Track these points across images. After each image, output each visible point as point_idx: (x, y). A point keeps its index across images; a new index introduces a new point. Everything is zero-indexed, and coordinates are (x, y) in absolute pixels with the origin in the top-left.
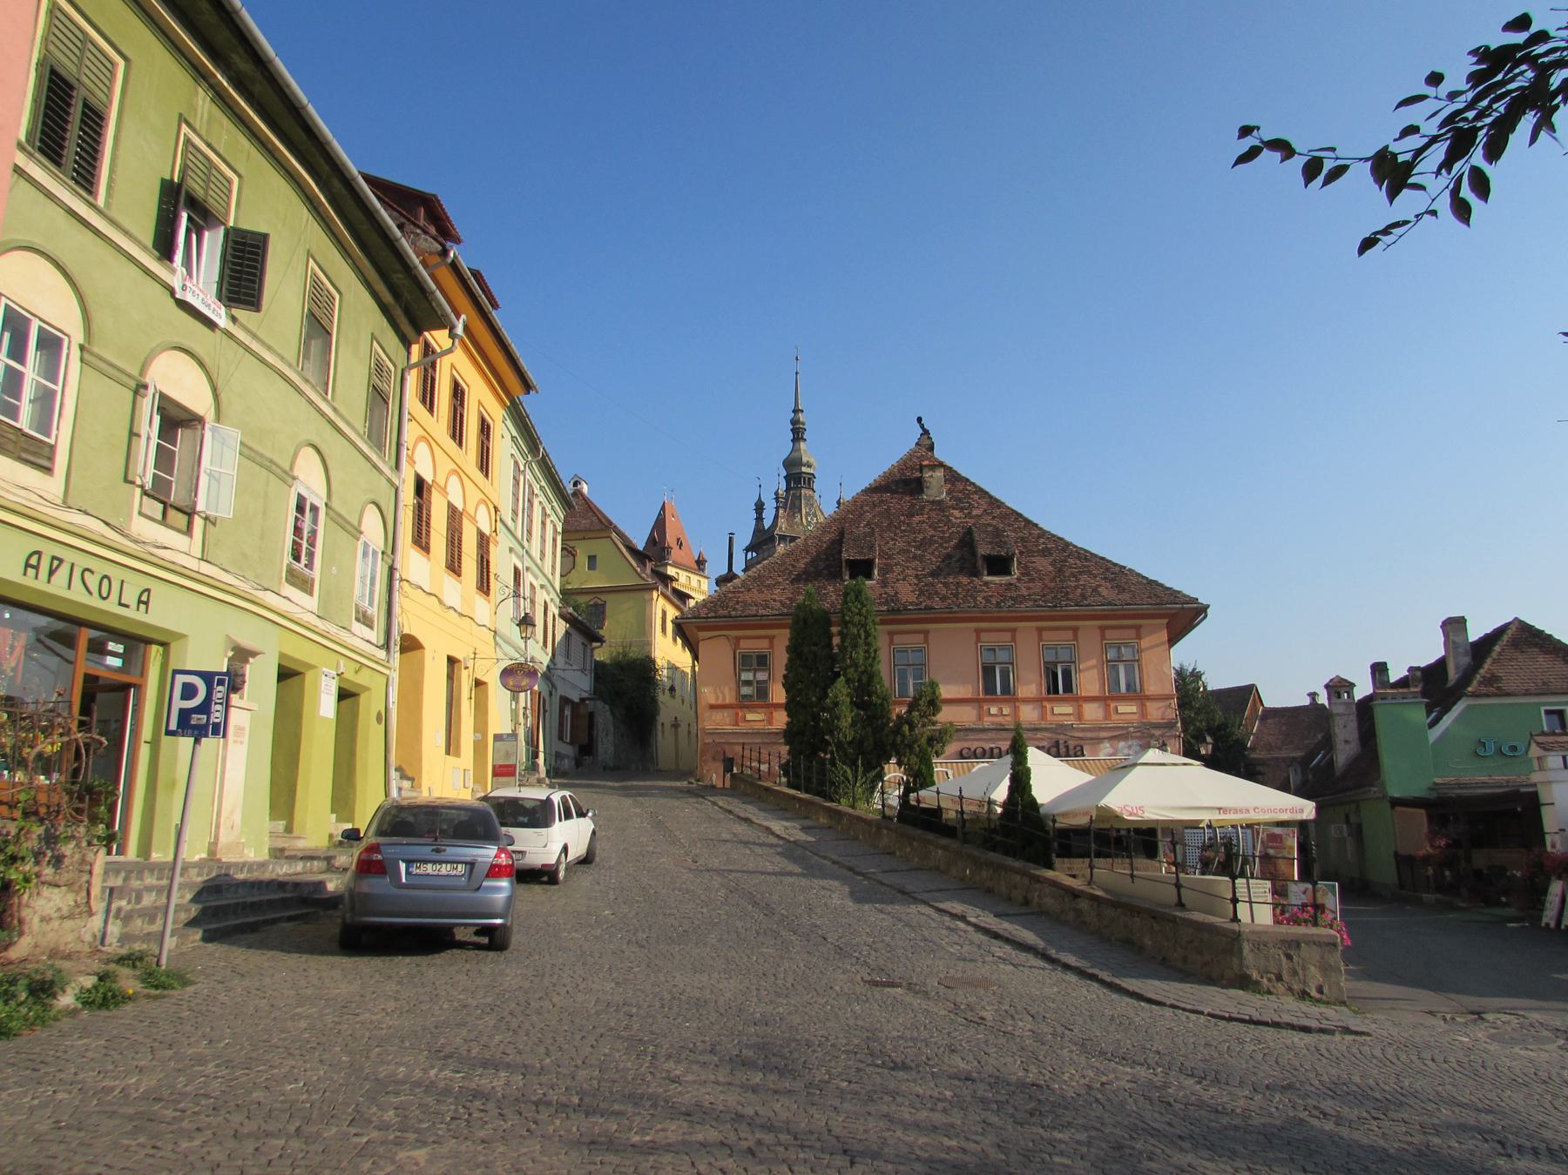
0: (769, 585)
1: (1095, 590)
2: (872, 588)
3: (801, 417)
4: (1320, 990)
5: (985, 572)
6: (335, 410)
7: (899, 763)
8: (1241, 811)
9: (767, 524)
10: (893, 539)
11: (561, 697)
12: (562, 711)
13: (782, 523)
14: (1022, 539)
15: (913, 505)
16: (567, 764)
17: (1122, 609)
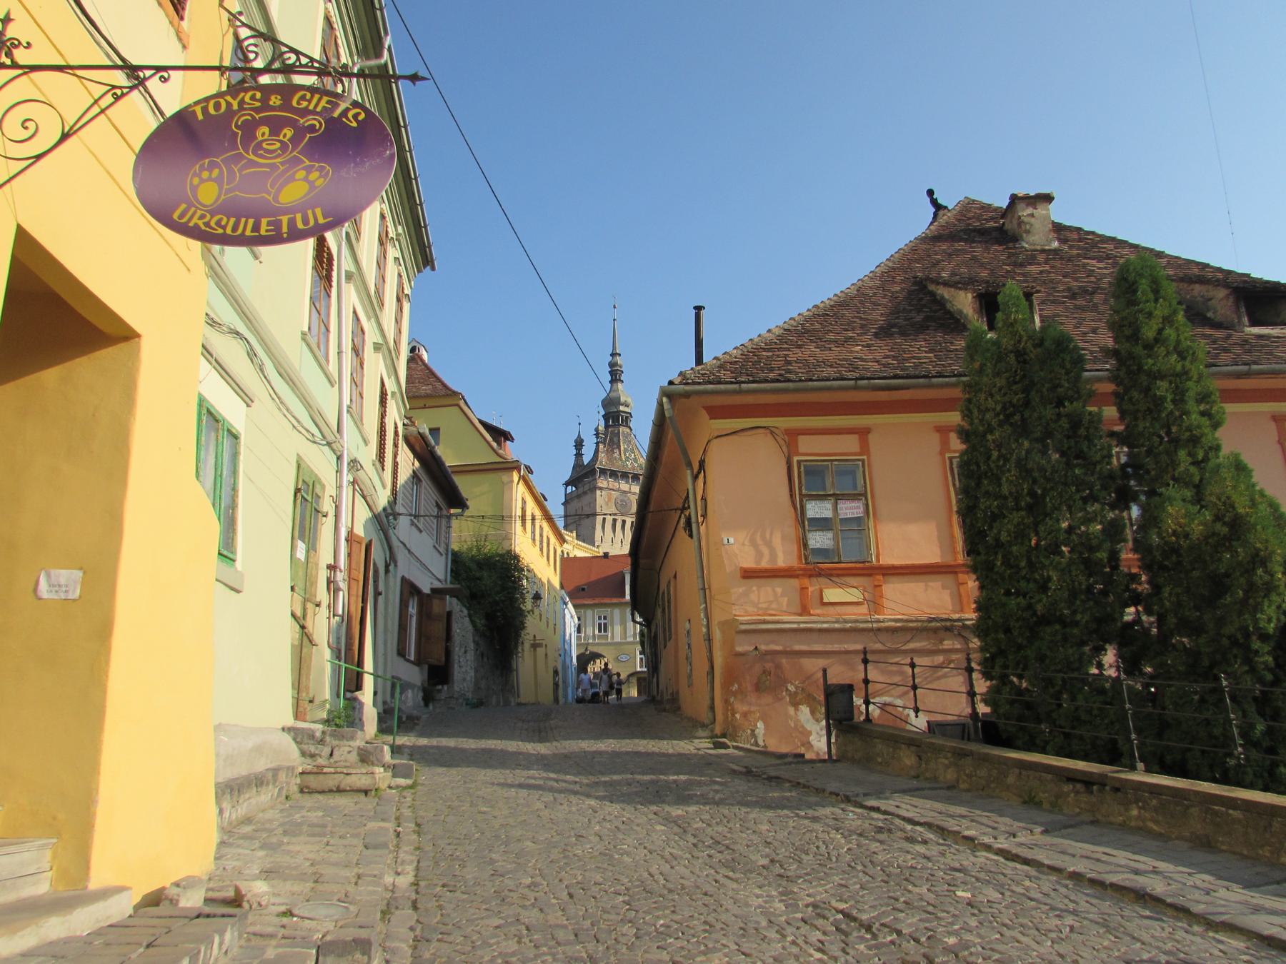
3: (619, 360)
5: (1246, 320)
9: (586, 460)
11: (403, 579)
12: (404, 605)
16: (412, 698)
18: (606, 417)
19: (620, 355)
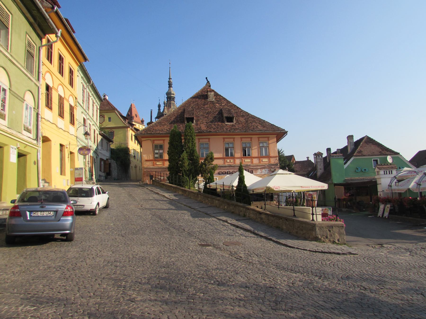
0: (163, 125)
1: (257, 127)
2: (193, 126)
3: (171, 80)
4: (338, 240)
5: (226, 122)
6: (11, 56)
7: (202, 176)
8: (306, 187)
9: (162, 111)
10: (199, 112)
11: (100, 158)
13: (166, 110)
14: (236, 112)
15: (205, 102)
16: (102, 178)
17: (264, 132)
18: (167, 98)
19: (171, 79)
